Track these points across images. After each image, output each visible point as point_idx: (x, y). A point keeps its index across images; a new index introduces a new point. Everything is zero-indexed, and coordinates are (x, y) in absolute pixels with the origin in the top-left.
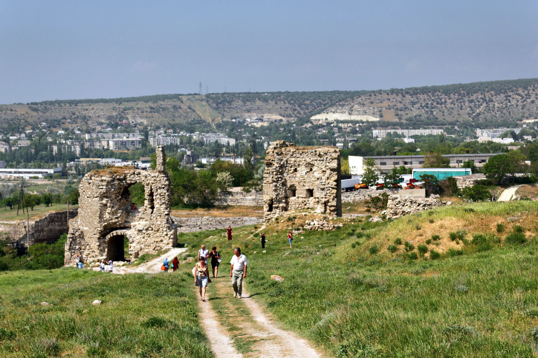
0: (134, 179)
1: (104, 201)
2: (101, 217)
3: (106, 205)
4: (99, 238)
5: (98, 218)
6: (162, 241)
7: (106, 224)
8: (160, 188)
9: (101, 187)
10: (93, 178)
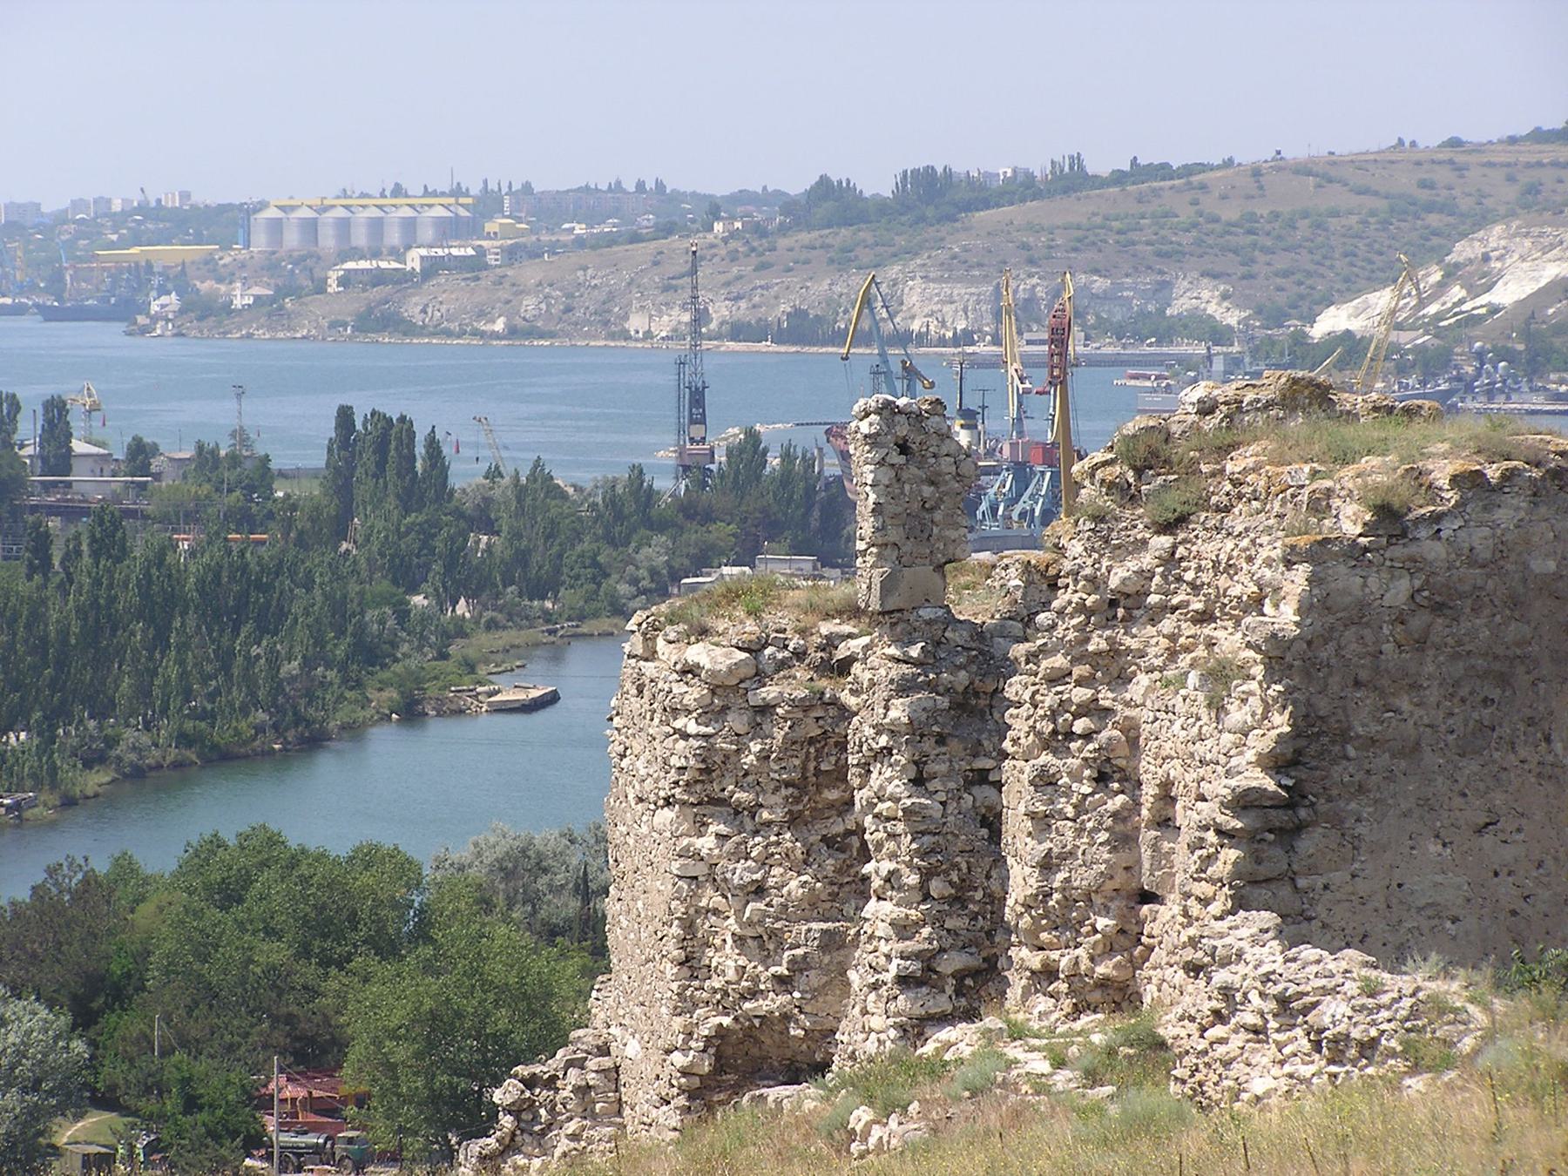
1: (706, 843)
2: (691, 964)
5: (670, 970)
7: (727, 1021)
9: (678, 724)
10: (660, 643)
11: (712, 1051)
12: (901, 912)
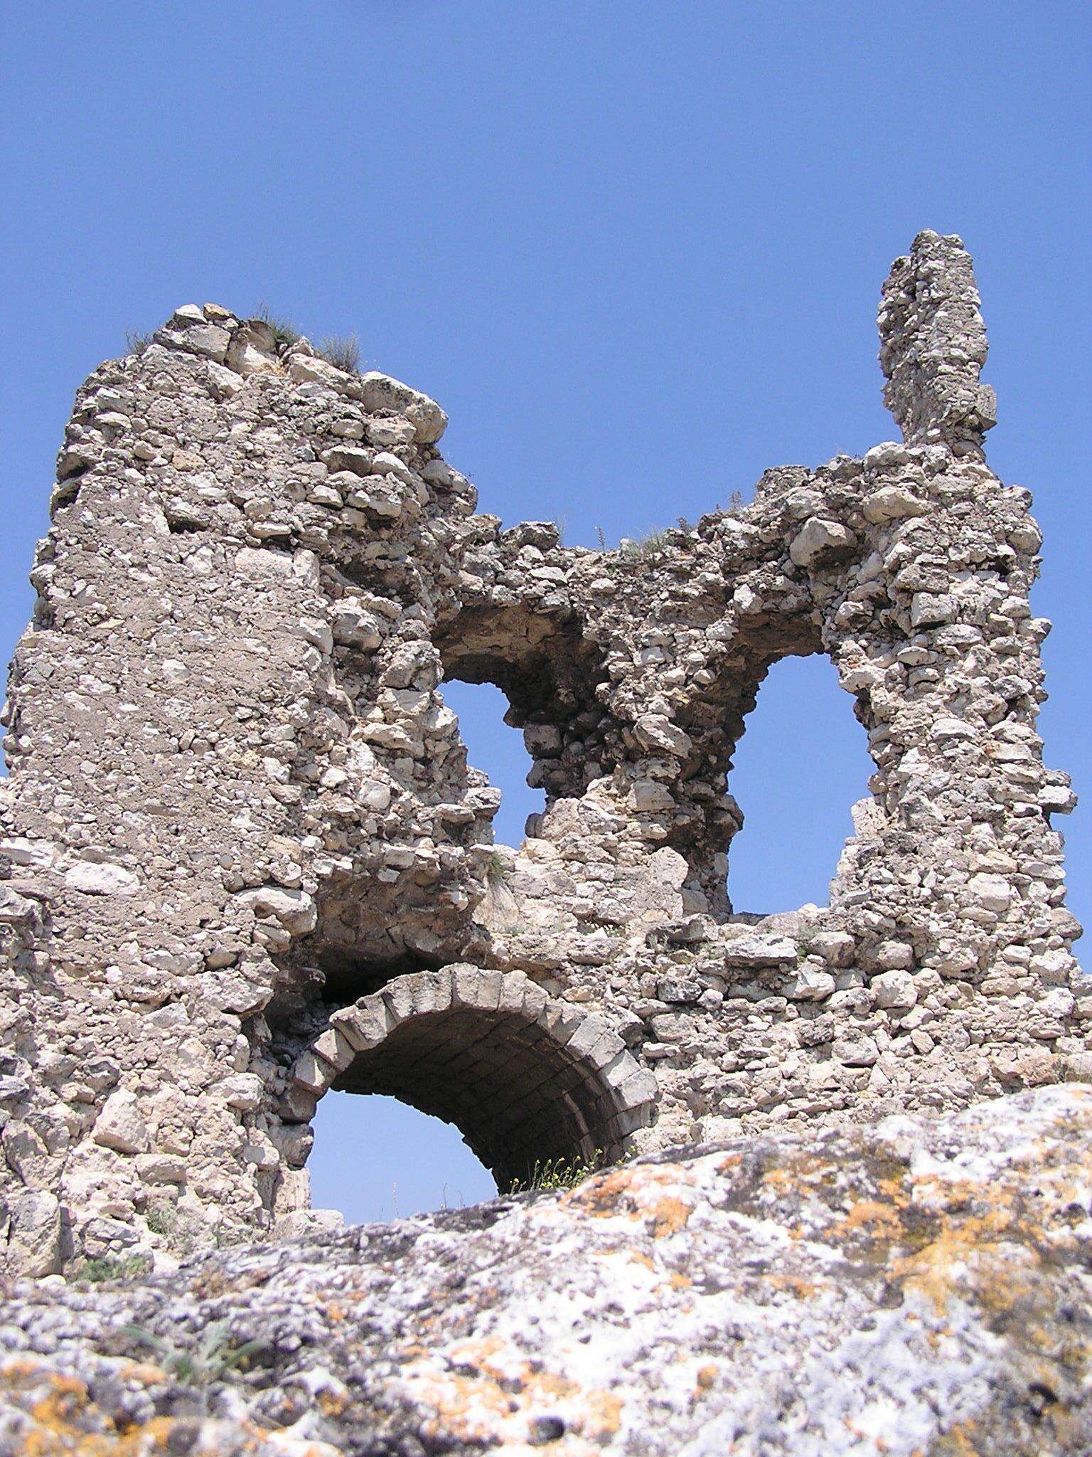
0: (513, 575)
7: (346, 863)
8: (971, 566)
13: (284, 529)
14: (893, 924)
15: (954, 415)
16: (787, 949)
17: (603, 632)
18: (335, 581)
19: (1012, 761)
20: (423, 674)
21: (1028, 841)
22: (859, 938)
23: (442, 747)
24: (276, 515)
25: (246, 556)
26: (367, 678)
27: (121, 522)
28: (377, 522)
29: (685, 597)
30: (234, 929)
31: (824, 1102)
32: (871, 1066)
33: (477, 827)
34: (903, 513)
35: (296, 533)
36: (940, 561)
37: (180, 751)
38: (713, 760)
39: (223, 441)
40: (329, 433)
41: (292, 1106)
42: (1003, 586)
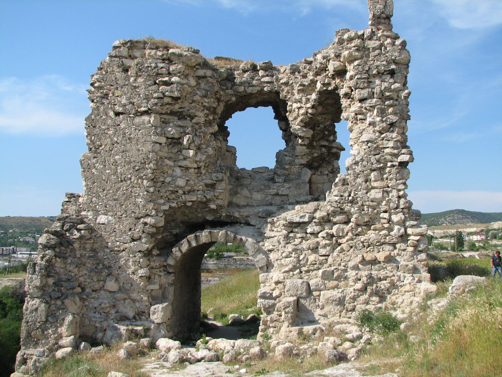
3: (175, 142)
4: (148, 254)
6: (390, 259)
7: (174, 205)
8: (380, 74)
9: (166, 79)
11: (164, 217)
12: (399, 138)
13: (146, 109)
14: (339, 209)
15: (375, 16)
16: (306, 219)
17: (286, 97)
18: (165, 119)
19: (388, 147)
20: (191, 145)
21: (391, 176)
22: (328, 214)
23: (202, 164)
24: (143, 105)
25: (137, 120)
26: (179, 146)
27: (102, 117)
28: (176, 99)
29: (304, 85)
30: (138, 230)
31: (312, 268)
32: (328, 256)
33: (217, 184)
34: (353, 59)
35: (149, 109)
36: (364, 77)
37: (122, 181)
38: (326, 133)
39: (127, 85)
40: (158, 74)
41: (168, 269)
42: (391, 81)
